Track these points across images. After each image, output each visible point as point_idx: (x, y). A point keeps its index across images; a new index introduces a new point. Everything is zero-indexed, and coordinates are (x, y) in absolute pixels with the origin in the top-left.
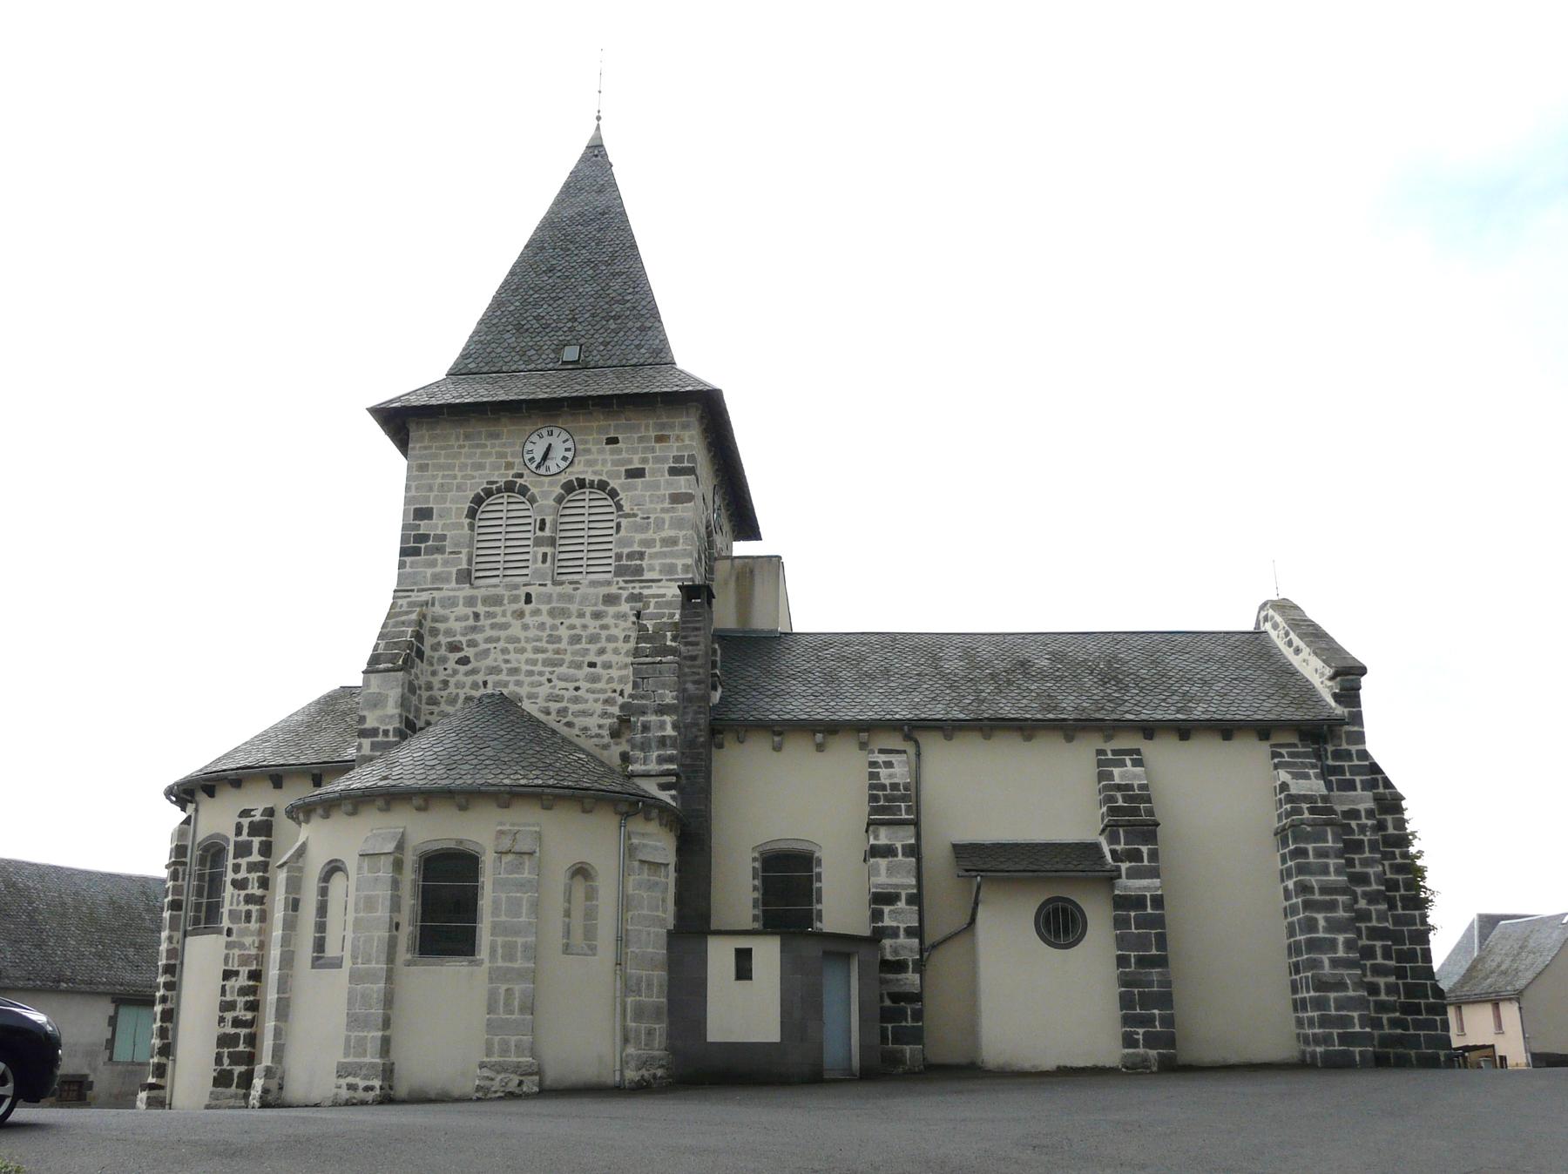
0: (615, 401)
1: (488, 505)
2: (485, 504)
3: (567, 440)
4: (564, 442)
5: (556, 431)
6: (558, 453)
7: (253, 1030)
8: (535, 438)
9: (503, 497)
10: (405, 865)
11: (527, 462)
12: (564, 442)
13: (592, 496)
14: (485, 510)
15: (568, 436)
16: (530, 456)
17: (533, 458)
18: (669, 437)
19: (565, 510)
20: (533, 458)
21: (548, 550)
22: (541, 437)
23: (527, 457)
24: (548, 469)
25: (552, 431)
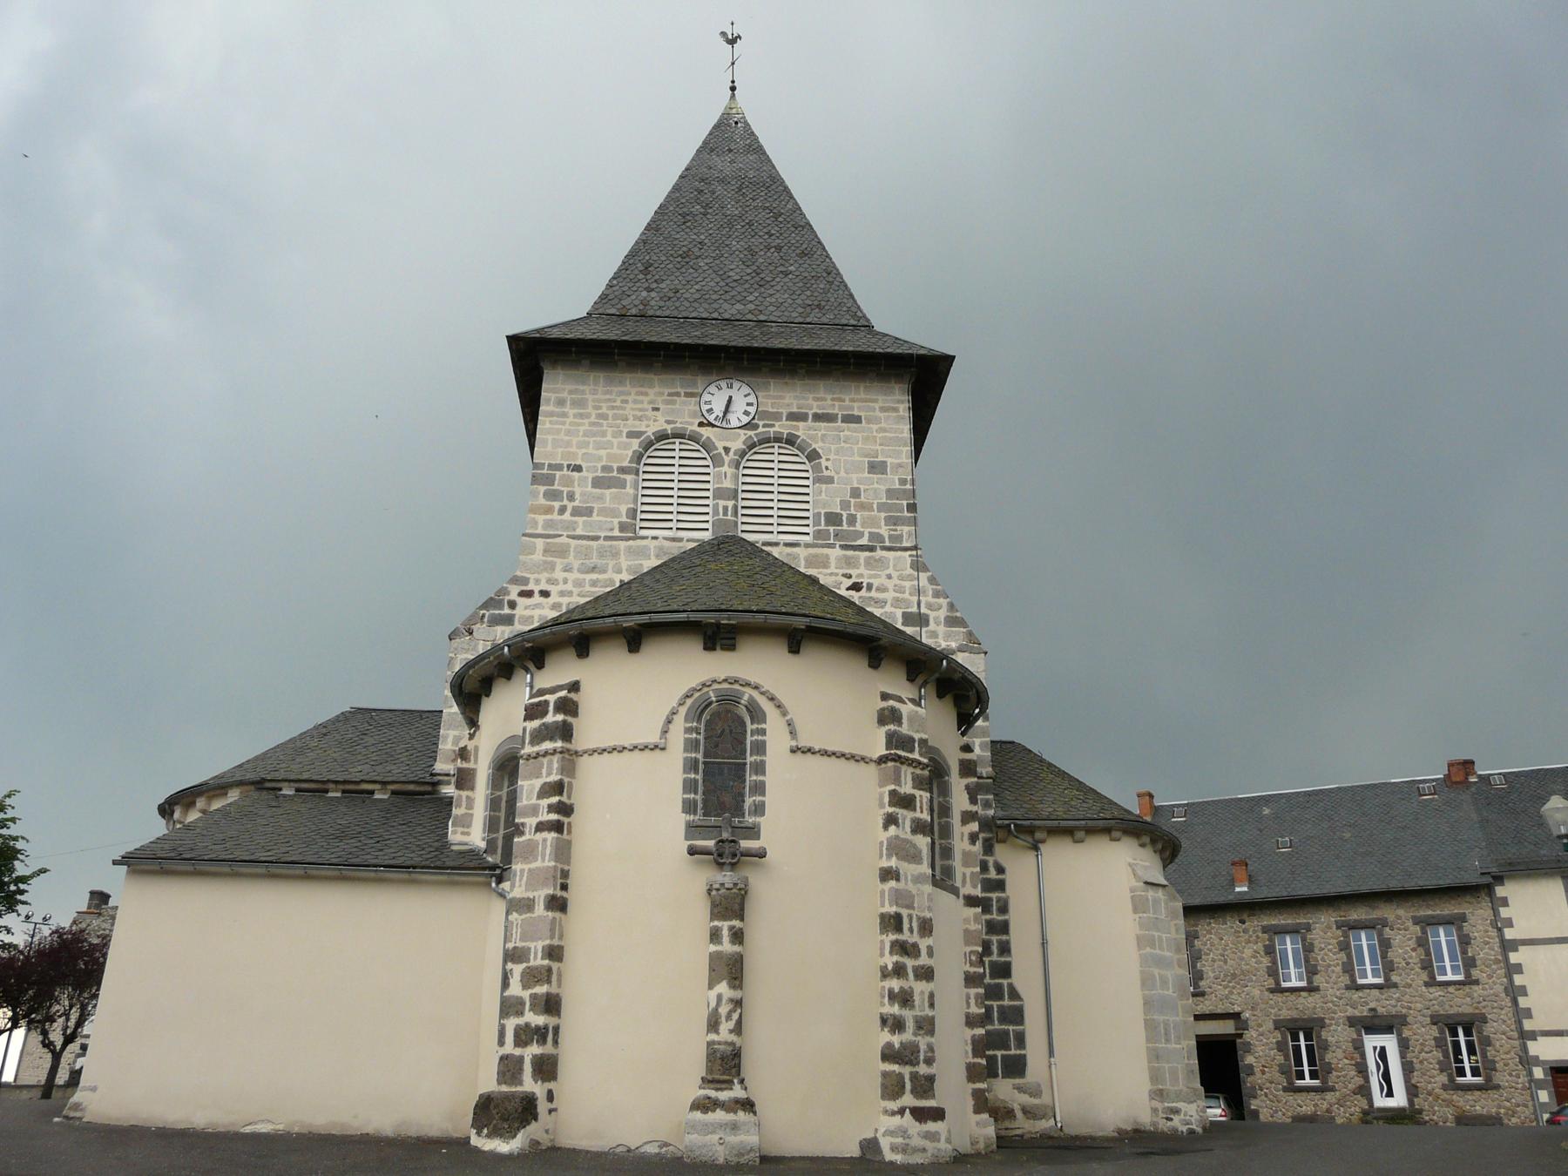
0: (883, 362)
1: (756, 453)
2: (653, 448)
3: (749, 394)
4: (745, 396)
5: (736, 385)
6: (739, 406)
7: (549, 1048)
8: (712, 389)
9: (774, 447)
10: (960, 818)
11: (705, 413)
12: (745, 396)
13: (782, 451)
14: (651, 455)
15: (750, 391)
16: (708, 407)
17: (711, 409)
18: (878, 399)
19: (748, 462)
20: (711, 409)
21: (730, 504)
22: (719, 388)
23: (705, 408)
24: (728, 422)
25: (732, 384)
